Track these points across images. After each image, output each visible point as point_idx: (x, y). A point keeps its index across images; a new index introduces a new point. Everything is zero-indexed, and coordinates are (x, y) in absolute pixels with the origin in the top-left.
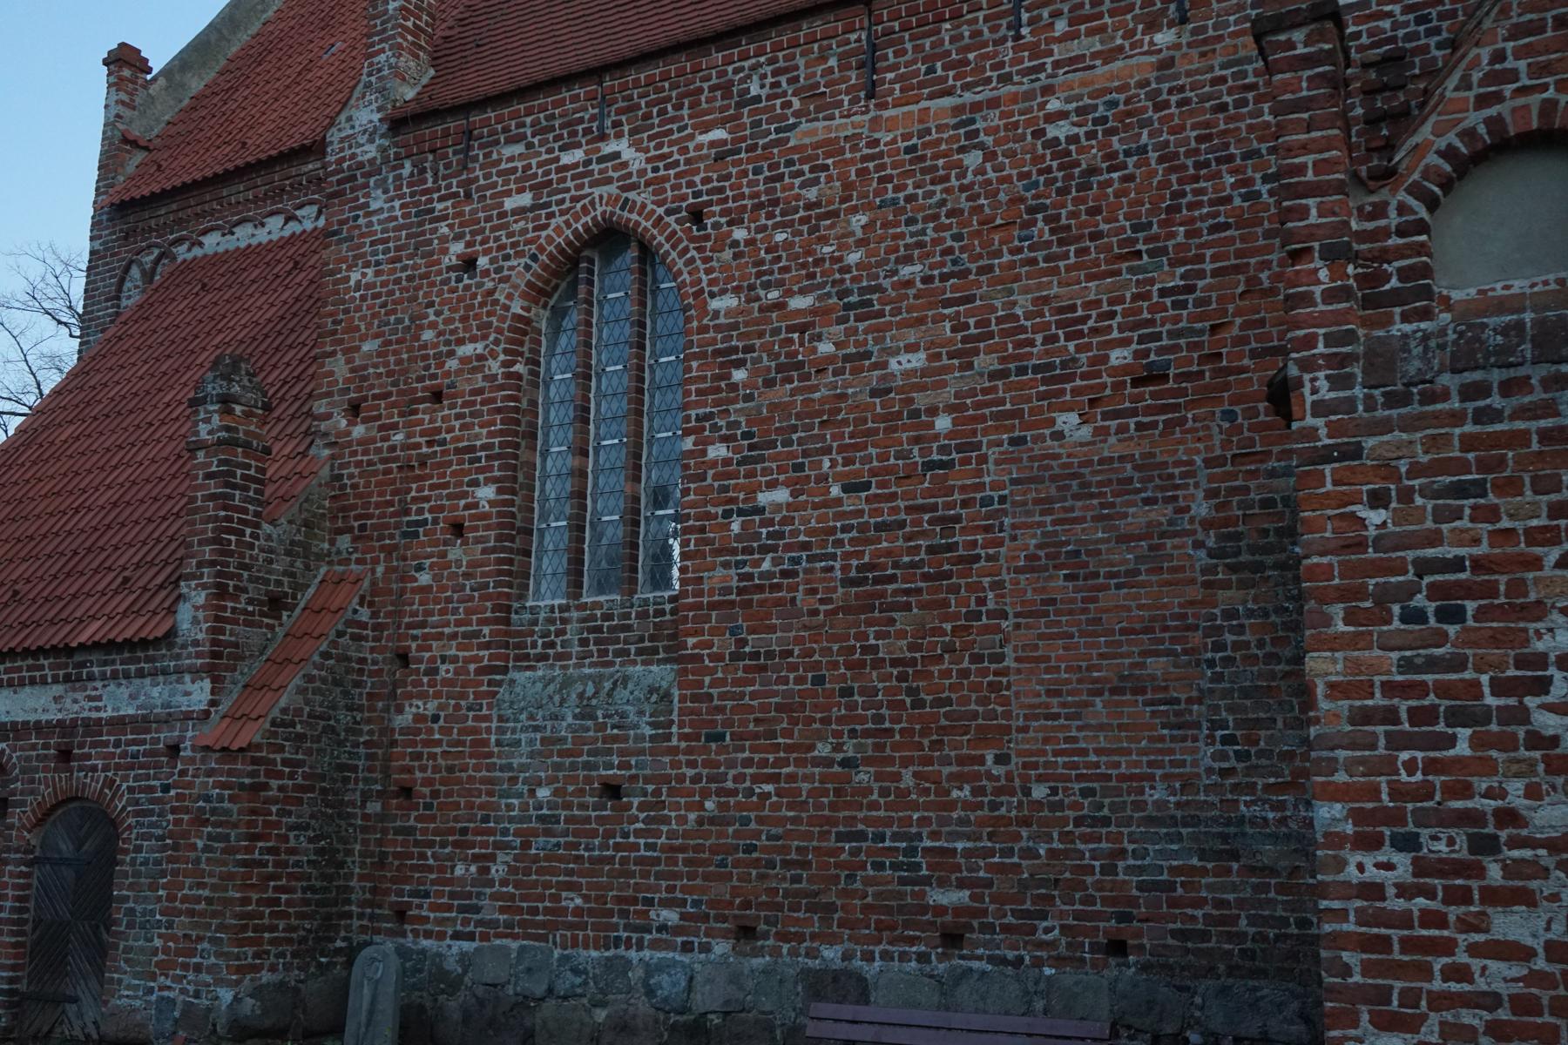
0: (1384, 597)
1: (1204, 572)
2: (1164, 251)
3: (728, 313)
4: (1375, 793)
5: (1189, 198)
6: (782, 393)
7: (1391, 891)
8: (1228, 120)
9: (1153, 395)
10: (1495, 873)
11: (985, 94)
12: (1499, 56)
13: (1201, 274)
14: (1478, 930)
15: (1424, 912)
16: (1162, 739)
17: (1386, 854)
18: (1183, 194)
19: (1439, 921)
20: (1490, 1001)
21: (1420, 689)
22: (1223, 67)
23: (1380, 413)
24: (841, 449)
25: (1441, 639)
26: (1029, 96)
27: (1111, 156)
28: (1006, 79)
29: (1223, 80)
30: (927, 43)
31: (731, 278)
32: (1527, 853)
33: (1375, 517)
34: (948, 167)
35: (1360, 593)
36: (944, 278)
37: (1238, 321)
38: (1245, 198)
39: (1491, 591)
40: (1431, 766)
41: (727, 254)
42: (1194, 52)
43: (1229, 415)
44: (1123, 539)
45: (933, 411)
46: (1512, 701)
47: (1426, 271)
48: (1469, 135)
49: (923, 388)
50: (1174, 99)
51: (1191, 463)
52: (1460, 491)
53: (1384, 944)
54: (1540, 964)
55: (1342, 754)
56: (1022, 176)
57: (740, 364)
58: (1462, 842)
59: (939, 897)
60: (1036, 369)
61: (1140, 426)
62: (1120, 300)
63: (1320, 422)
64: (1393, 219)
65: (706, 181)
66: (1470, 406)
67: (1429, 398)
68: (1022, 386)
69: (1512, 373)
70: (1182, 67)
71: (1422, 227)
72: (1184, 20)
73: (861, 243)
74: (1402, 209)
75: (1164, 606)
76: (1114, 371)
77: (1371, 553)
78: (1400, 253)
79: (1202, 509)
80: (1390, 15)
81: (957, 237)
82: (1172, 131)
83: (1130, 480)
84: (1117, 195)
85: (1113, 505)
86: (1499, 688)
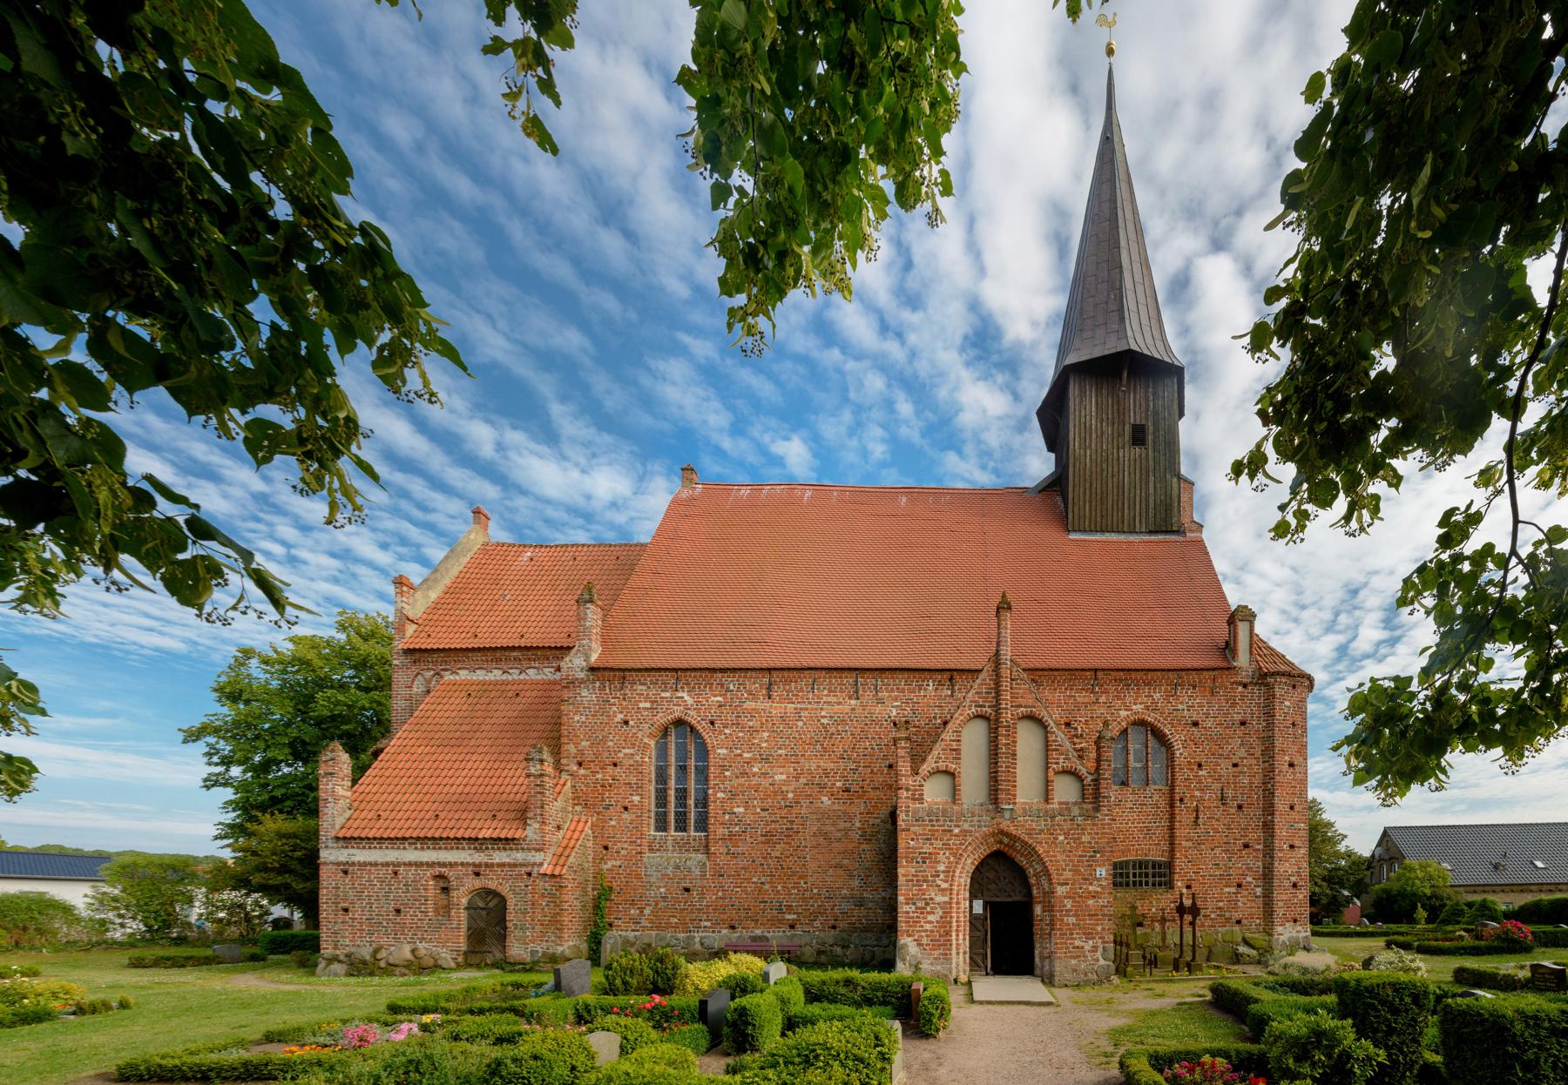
6: (741, 781)
59: (788, 917)
79: (858, 825)
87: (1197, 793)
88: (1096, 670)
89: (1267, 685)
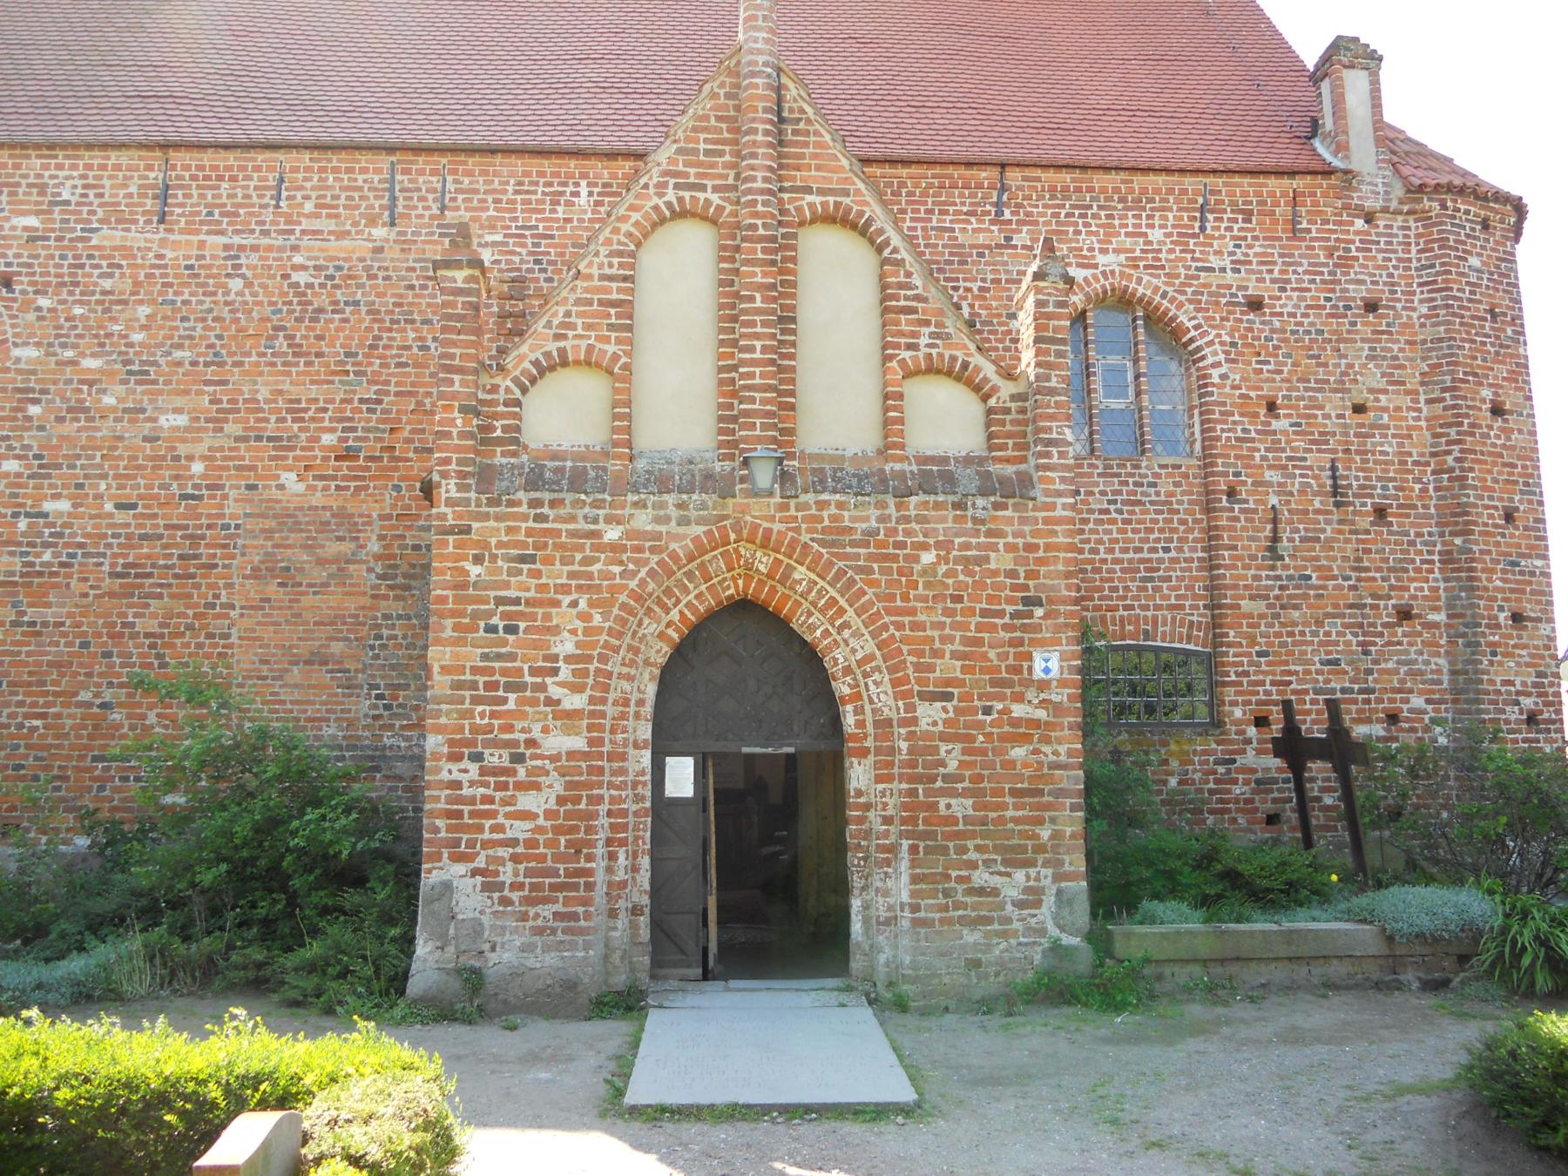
0: (476, 616)
1: (374, 587)
2: (364, 373)
3: (29, 361)
4: (461, 729)
5: (385, 341)
6: (69, 428)
7: (466, 784)
8: (416, 296)
9: (349, 468)
10: (522, 773)
11: (249, 241)
12: (568, 314)
13: (387, 393)
14: (510, 804)
15: (483, 796)
16: (336, 695)
17: (466, 764)
18: (380, 338)
19: (490, 800)
20: (514, 842)
21: (491, 672)
22: (415, 261)
23: (484, 509)
24: (116, 477)
25: (505, 643)
26: (281, 249)
27: (336, 303)
28: (265, 233)
29: (414, 269)
30: (209, 193)
31: (32, 335)
32: (539, 763)
33: (475, 571)
34: (217, 285)
35: (462, 614)
36: (206, 364)
37: (408, 428)
38: (421, 348)
39: (533, 617)
40: (493, 715)
41: (31, 316)
42: (398, 247)
43: (397, 488)
44: (321, 562)
45: (190, 458)
46: (539, 680)
47: (518, 429)
48: (547, 355)
49: (184, 440)
50: (381, 274)
51: (369, 516)
52: (523, 559)
53: (459, 814)
54: (541, 821)
55: (444, 707)
56: (271, 303)
57: (36, 401)
58: (506, 757)
60: (270, 439)
61: (338, 488)
62: (332, 401)
63: (448, 510)
64: (501, 396)
65: (17, 256)
66: (533, 512)
67: (511, 503)
68: (257, 449)
69: (556, 495)
70: (387, 254)
71: (518, 403)
72: (393, 224)
73: (144, 328)
74: (508, 390)
75: (346, 608)
76: (323, 448)
77: (471, 591)
78: (503, 416)
79: (375, 547)
80: (519, 254)
81: (219, 337)
82: (378, 295)
83: (328, 523)
84: (337, 330)
85: (315, 539)
86: (534, 672)
87: (1271, 476)
88: (1003, 166)
89: (1423, 216)
